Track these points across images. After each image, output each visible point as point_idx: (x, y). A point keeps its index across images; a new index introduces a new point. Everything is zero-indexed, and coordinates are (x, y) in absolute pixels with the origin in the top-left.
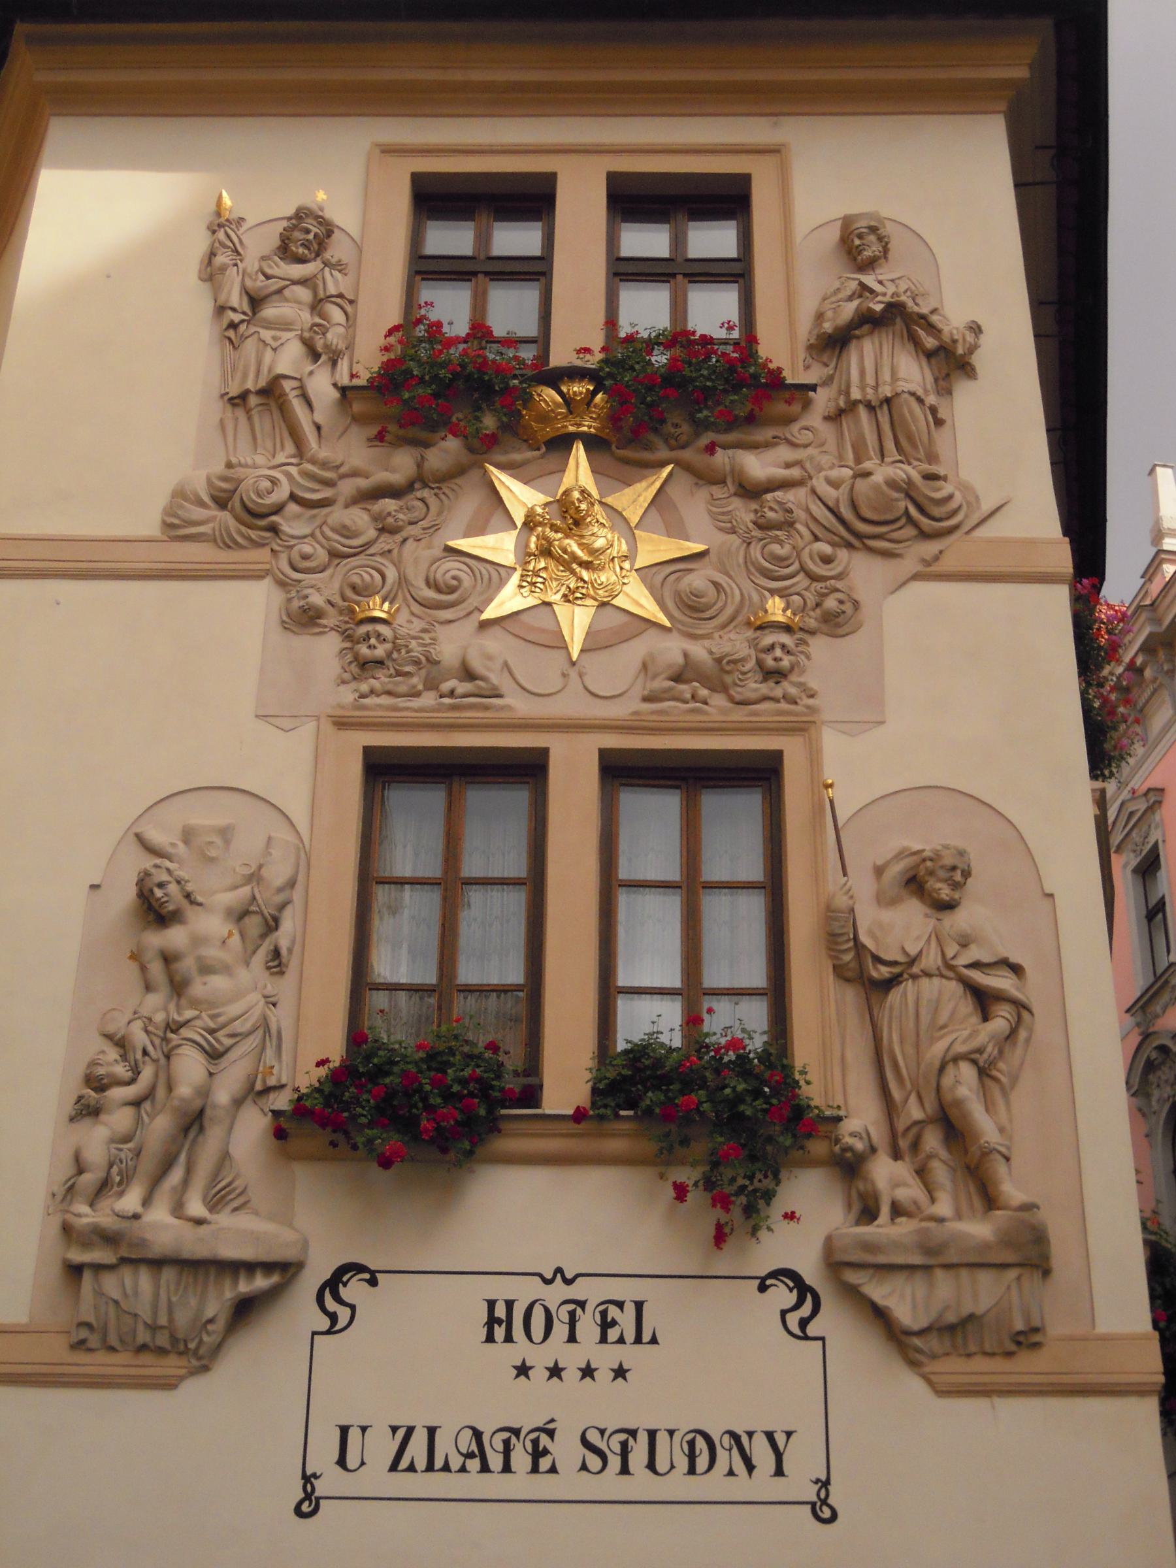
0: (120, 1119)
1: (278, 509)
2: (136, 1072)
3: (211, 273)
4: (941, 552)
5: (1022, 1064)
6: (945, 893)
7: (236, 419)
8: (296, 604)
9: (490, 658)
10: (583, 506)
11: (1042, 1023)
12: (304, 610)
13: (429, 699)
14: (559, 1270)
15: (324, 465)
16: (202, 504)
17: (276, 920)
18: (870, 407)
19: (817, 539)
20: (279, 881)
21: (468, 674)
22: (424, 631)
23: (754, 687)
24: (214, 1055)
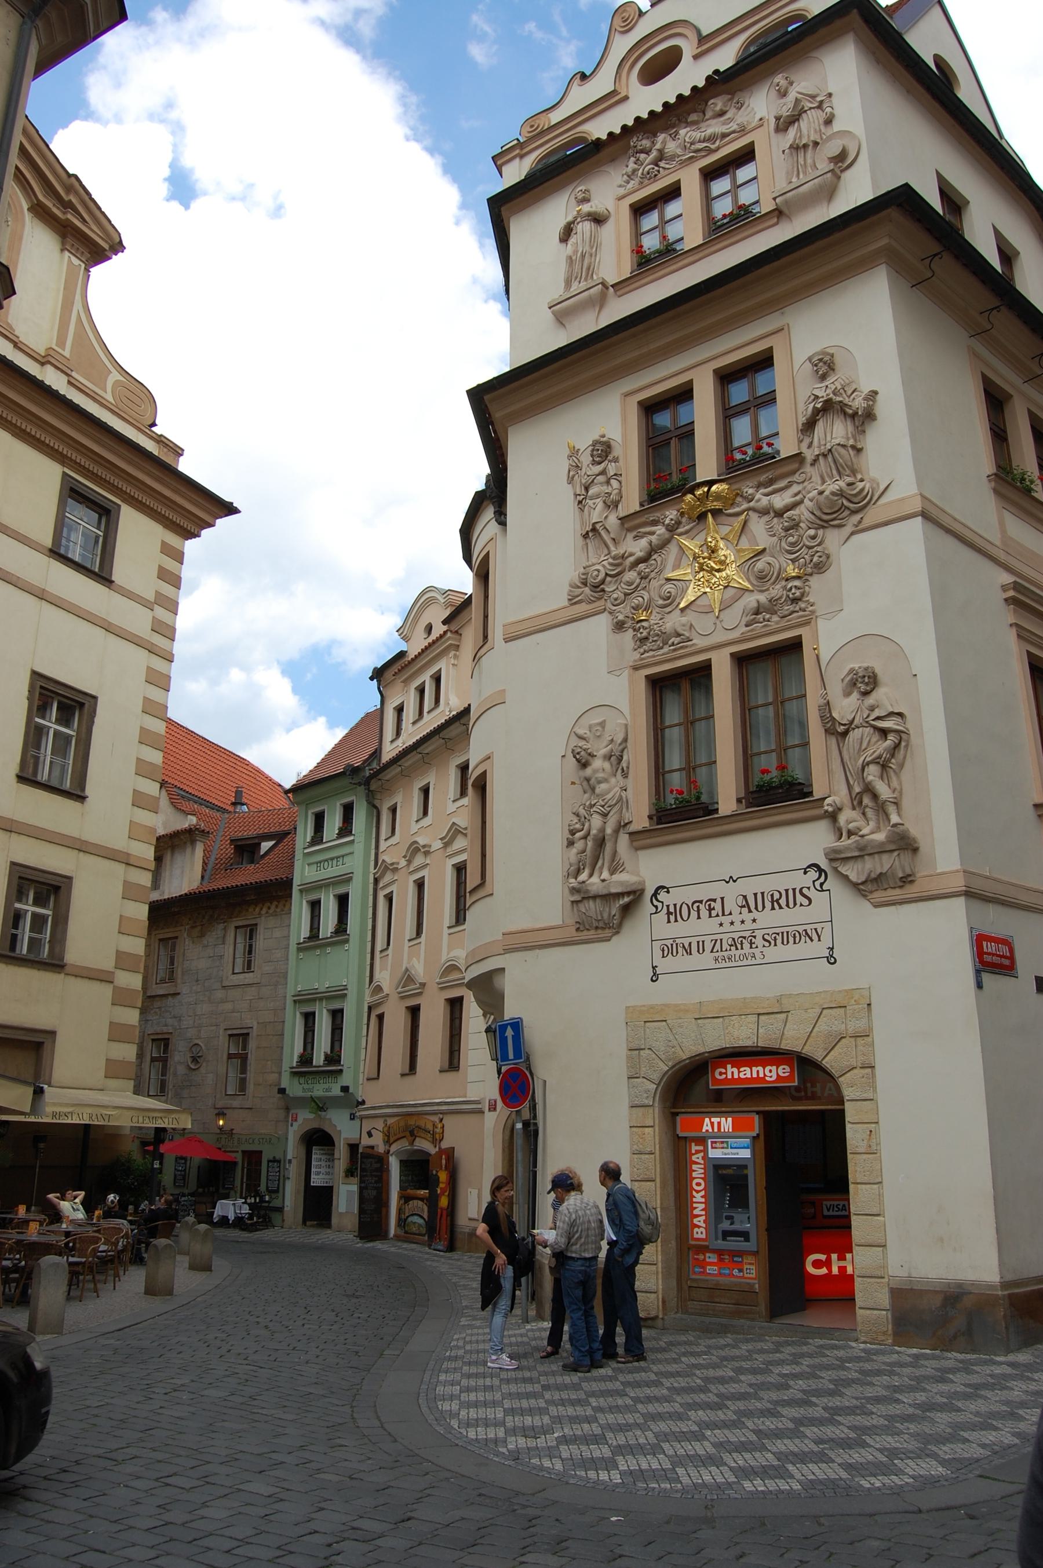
0: (579, 845)
1: (603, 582)
2: (584, 825)
3: (571, 480)
4: (862, 518)
5: (905, 758)
6: (863, 687)
7: (587, 544)
8: (615, 620)
9: (684, 625)
10: (713, 544)
11: (914, 740)
12: (617, 623)
13: (666, 649)
14: (731, 877)
15: (614, 558)
16: (579, 587)
17: (622, 756)
18: (825, 456)
19: (810, 528)
20: (619, 741)
21: (679, 635)
22: (661, 619)
23: (788, 608)
24: (605, 815)
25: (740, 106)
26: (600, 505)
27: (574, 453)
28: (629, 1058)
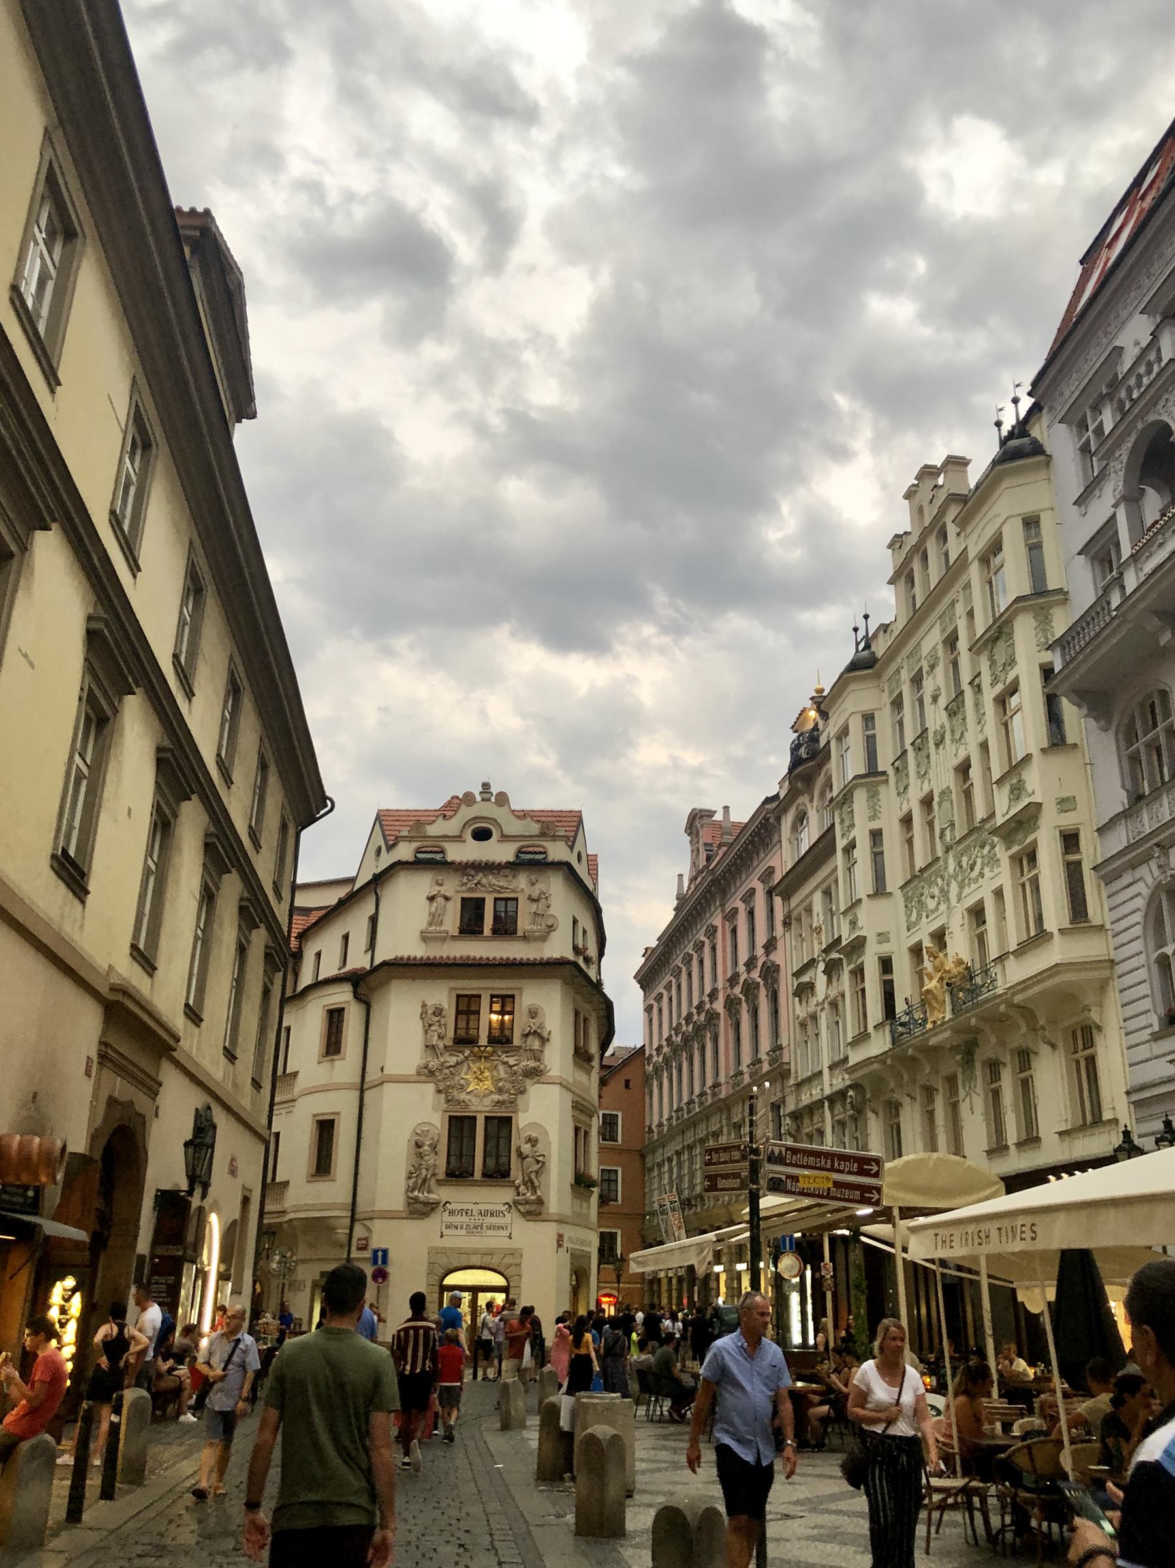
0: (414, 1180)
25: (514, 876)
26: (436, 1037)
27: (424, 1006)
28: (428, 1268)
